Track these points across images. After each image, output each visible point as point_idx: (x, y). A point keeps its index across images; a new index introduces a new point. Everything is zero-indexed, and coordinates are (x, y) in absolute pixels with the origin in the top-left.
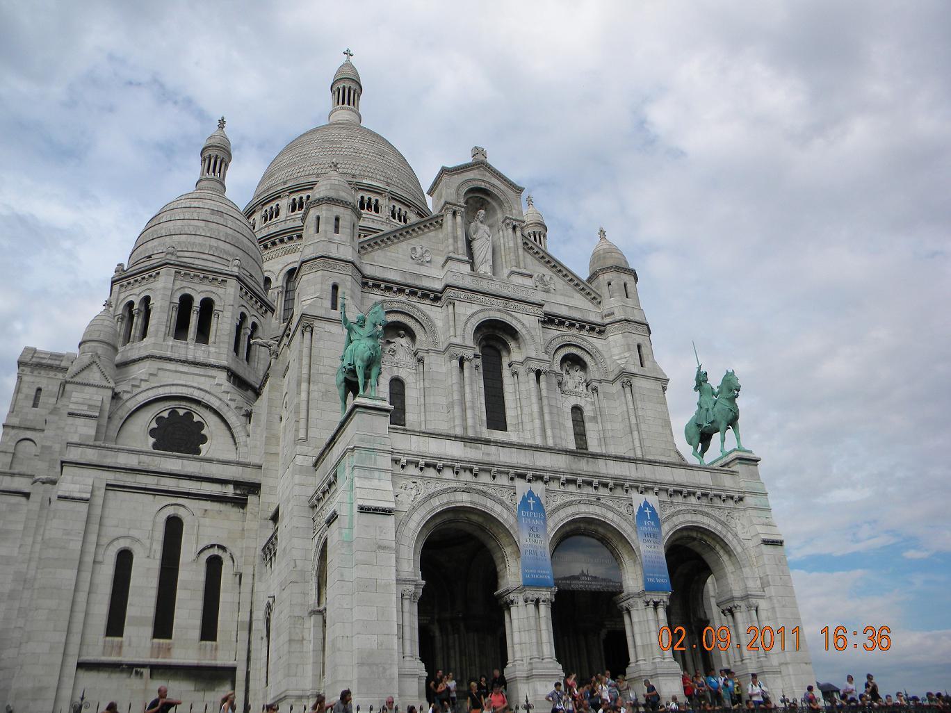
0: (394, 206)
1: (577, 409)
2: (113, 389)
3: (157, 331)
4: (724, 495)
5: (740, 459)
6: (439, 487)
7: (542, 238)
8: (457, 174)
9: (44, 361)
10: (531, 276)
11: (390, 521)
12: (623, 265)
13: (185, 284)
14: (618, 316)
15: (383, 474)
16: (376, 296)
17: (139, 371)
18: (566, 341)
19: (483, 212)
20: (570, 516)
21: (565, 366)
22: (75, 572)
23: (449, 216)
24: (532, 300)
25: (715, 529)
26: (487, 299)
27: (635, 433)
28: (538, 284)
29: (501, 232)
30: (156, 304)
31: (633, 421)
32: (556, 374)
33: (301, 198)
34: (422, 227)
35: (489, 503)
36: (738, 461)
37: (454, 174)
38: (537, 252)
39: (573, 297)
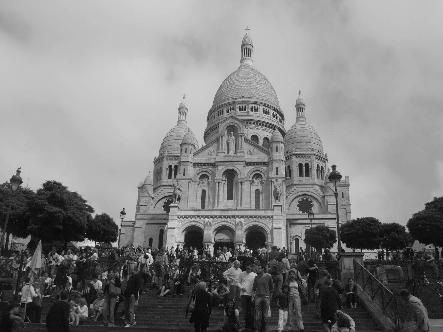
0: (252, 107)
1: (257, 190)
2: (151, 197)
4: (266, 216)
6: (188, 221)
7: (302, 109)
10: (244, 152)
12: (278, 140)
13: (169, 162)
15: (175, 220)
16: (198, 168)
19: (232, 133)
23: (221, 138)
24: (241, 160)
25: (262, 226)
27: (271, 196)
28: (248, 152)
31: (271, 193)
32: (250, 181)
34: (213, 143)
35: (199, 224)
39: (261, 154)
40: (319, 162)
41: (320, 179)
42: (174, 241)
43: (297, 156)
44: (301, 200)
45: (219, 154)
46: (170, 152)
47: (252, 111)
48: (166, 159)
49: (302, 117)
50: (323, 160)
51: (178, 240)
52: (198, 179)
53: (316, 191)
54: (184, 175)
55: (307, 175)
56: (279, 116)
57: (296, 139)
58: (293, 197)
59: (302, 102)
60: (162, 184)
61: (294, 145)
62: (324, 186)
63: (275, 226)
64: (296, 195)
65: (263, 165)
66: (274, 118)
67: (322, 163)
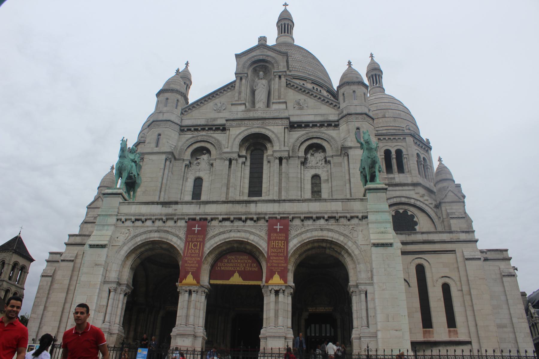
1: (316, 177)
4: (348, 216)
5: (370, 189)
6: (142, 230)
7: (377, 77)
8: (245, 55)
10: (286, 103)
11: (105, 250)
12: (355, 80)
14: (345, 113)
16: (188, 135)
18: (310, 136)
19: (261, 73)
20: (223, 240)
21: (311, 151)
22: (65, 294)
23: (238, 81)
24: (281, 117)
25: (338, 240)
26: (251, 122)
29: (273, 82)
32: (299, 157)
34: (222, 91)
35: (170, 237)
36: (367, 191)
37: (243, 56)
38: (297, 87)
40: (419, 150)
41: (423, 178)
42: (100, 279)
45: (234, 108)
49: (380, 87)
50: (425, 148)
51: (113, 276)
52: (187, 155)
53: (421, 197)
63: (375, 238)
65: (326, 127)
67: (422, 152)
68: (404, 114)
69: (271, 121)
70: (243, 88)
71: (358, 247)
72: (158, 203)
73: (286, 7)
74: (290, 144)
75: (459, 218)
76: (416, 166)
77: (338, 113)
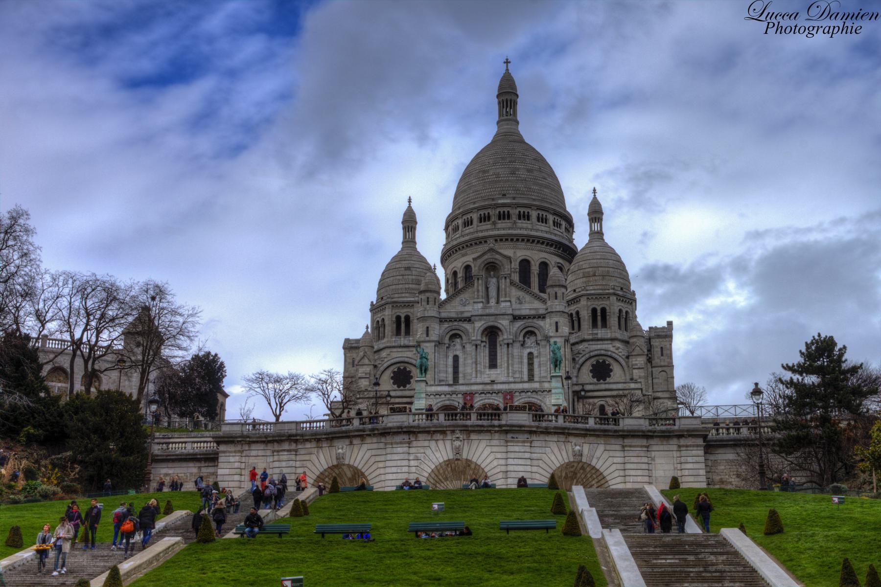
0: (520, 212)
1: (530, 354)
2: (373, 365)
3: (388, 335)
5: (553, 376)
6: (440, 400)
9: (353, 345)
10: (510, 301)
13: (396, 311)
14: (549, 310)
16: (446, 325)
17: (384, 354)
19: (492, 273)
21: (527, 336)
28: (518, 301)
29: (500, 281)
30: (387, 322)
32: (519, 341)
33: (468, 218)
40: (622, 305)
43: (589, 297)
44: (595, 363)
45: (476, 305)
46: (396, 295)
47: (520, 219)
48: (391, 306)
52: (447, 341)
54: (427, 335)
55: (605, 325)
56: (563, 223)
57: (587, 270)
58: (584, 359)
59: (597, 208)
60: (388, 345)
61: (584, 279)
62: (627, 339)
64: (587, 356)
66: (556, 228)
67: (626, 306)
68: (613, 270)
69: (501, 316)
70: (480, 288)
71: (546, 406)
72: (446, 385)
73: (507, 66)
74: (514, 331)
75: (639, 368)
76: (617, 323)
77: (544, 307)
